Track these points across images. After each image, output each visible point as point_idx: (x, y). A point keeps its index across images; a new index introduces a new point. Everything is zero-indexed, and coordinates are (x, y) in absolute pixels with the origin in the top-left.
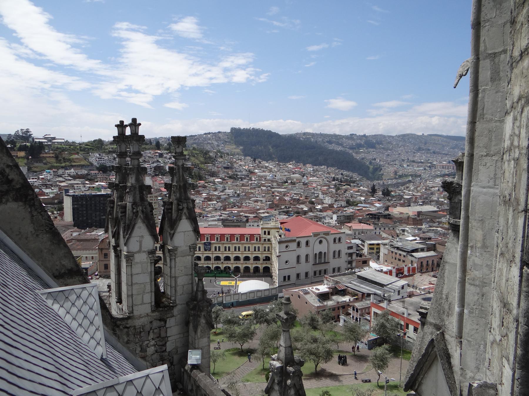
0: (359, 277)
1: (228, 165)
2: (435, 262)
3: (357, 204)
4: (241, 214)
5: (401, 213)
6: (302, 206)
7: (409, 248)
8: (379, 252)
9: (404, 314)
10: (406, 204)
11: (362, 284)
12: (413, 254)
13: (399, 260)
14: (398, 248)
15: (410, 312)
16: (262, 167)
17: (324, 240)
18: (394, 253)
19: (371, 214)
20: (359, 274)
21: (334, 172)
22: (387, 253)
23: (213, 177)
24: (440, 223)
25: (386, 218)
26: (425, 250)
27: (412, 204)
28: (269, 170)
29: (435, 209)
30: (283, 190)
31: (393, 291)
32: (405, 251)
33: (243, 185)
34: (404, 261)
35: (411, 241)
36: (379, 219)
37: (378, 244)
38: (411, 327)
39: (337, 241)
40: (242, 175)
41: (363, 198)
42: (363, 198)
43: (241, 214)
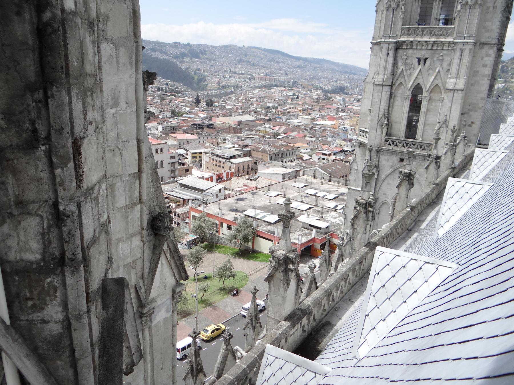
0: (181, 185)
2: (250, 167)
3: (182, 115)
5: (224, 123)
7: (228, 154)
8: (201, 161)
9: (218, 214)
10: (228, 115)
11: (183, 191)
12: (231, 160)
13: (219, 166)
14: (218, 156)
15: (223, 212)
18: (215, 161)
19: (196, 125)
20: (180, 182)
22: (208, 161)
24: (256, 131)
26: (242, 156)
27: (233, 114)
29: (253, 118)
31: (211, 195)
32: (224, 158)
36: (203, 128)
37: (201, 153)
38: (225, 225)
39: (159, 151)
41: (188, 109)
42: (188, 109)
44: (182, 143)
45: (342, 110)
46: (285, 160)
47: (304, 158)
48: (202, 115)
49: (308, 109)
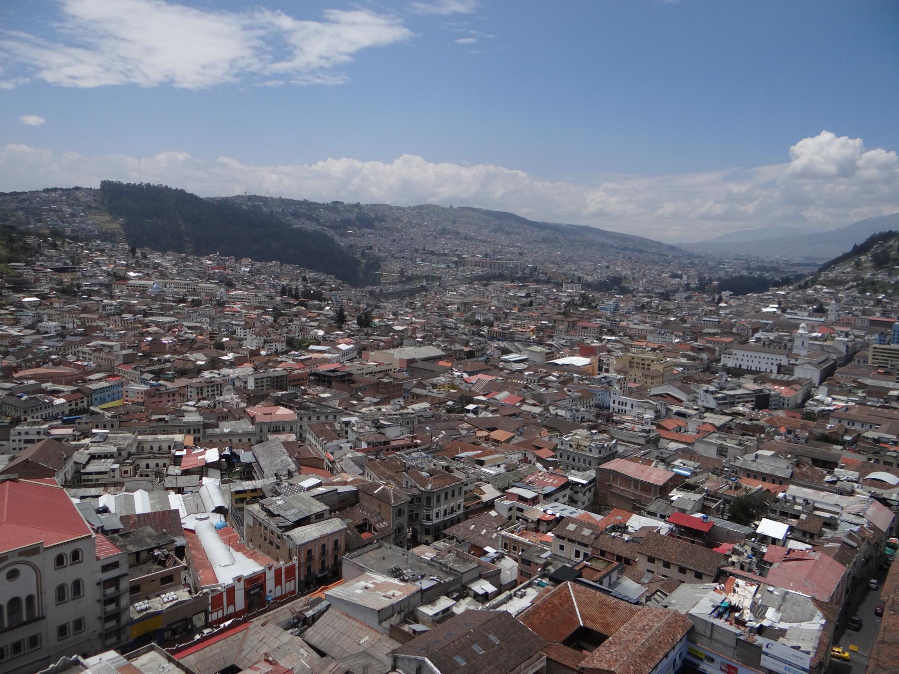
1: (66, 264)
3: (309, 346)
4: (44, 385)
6: (192, 357)
16: (147, 266)
17: (19, 567)
21: (290, 276)
23: (21, 291)
24: (434, 386)
25: (344, 381)
27: (405, 342)
28: (159, 275)
29: (439, 352)
30: (168, 319)
33: (85, 310)
34: (278, 547)
35: (309, 488)
39: (68, 560)
40: (95, 285)
41: (321, 333)
42: (321, 333)
43: (44, 385)
44: (265, 429)
45: (609, 331)
46: (435, 510)
47: (485, 498)
48: (343, 347)
49: (546, 326)
